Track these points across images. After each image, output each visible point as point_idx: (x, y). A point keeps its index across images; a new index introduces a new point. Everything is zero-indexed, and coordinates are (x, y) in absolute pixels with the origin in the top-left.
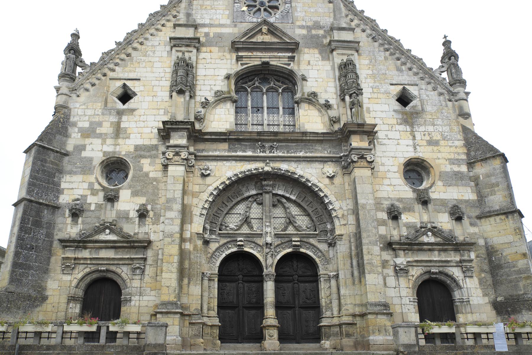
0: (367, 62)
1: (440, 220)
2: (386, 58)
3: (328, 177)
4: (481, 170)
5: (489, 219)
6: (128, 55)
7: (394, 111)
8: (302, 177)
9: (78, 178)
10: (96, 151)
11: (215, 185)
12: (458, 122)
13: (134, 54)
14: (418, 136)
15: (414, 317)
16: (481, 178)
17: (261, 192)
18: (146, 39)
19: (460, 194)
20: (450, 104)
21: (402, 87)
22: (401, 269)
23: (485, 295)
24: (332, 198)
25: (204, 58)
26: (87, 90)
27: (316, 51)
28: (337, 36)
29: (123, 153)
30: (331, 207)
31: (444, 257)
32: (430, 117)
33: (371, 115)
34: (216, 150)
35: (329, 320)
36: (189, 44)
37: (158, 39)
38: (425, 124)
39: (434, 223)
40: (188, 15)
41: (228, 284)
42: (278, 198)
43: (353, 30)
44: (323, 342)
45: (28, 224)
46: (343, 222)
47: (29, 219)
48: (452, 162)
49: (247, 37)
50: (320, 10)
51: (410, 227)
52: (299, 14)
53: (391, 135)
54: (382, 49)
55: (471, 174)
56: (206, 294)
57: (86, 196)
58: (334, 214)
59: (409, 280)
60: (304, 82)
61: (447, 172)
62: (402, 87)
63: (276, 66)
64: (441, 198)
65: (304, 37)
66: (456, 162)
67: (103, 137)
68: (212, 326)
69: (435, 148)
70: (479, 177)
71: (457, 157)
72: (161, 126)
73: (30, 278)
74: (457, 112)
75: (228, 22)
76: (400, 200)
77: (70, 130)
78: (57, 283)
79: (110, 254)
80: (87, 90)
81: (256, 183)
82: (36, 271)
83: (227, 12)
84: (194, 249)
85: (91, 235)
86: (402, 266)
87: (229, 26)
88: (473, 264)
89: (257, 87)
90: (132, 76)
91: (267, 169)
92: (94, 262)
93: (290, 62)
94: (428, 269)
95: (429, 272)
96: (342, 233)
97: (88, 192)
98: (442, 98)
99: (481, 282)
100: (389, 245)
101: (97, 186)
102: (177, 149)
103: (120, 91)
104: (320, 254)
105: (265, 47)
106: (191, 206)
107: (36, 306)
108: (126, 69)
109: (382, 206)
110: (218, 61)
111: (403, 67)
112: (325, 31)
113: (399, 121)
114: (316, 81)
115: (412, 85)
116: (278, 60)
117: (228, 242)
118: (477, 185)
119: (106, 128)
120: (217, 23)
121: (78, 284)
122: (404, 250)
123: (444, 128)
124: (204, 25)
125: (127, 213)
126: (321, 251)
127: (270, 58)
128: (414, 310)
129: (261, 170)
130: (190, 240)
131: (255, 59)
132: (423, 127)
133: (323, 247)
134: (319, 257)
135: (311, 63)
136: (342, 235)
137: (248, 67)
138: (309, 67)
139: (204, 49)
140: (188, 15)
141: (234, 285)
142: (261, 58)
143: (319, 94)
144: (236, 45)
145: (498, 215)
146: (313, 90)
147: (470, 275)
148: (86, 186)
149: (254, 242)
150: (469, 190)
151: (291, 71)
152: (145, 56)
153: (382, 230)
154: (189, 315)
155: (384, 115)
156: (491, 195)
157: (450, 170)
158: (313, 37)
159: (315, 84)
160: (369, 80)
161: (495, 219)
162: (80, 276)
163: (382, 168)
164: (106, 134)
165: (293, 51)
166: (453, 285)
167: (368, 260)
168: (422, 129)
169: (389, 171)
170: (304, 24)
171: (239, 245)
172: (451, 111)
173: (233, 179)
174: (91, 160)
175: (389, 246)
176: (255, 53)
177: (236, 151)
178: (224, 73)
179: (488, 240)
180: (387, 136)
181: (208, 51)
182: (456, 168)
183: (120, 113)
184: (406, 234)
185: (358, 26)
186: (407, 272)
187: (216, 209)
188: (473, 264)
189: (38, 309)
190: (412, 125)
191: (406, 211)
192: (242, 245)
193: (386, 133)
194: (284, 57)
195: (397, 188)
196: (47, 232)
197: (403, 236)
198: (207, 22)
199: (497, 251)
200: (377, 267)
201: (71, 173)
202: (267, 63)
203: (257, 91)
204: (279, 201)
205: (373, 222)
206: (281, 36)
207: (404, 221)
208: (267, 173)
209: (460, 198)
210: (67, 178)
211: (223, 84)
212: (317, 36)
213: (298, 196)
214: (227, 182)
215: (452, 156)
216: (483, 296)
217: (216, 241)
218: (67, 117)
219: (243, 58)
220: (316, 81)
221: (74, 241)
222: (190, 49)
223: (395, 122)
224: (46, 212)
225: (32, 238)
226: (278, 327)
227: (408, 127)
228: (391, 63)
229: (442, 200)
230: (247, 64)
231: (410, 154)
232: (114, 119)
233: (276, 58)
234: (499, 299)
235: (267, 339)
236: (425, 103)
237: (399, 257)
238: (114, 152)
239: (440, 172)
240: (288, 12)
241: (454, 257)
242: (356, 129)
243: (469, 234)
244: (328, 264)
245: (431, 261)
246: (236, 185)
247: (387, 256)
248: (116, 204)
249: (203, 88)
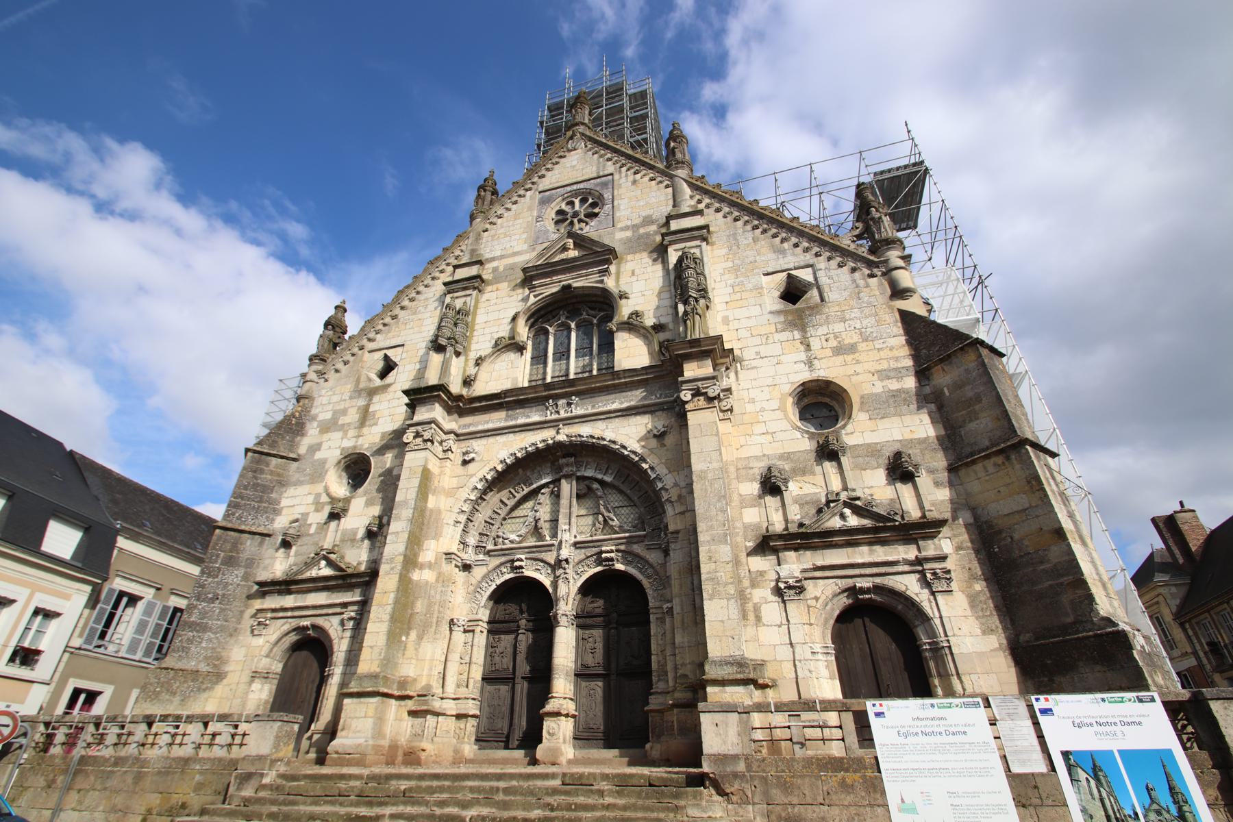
0: (725, 251)
1: (868, 483)
2: (755, 240)
3: (655, 436)
4: (943, 379)
5: (974, 467)
6: (394, 317)
7: (771, 313)
8: (614, 442)
9: (305, 489)
10: (333, 448)
11: (480, 475)
12: (891, 307)
13: (401, 314)
14: (815, 344)
15: (828, 687)
16: (947, 393)
17: (557, 476)
18: (418, 293)
19: (908, 430)
20: (873, 281)
21: (785, 274)
22: (790, 587)
23: (987, 631)
24: (662, 470)
26: (337, 371)
28: (675, 225)
29: (366, 446)
30: (660, 485)
31: (881, 553)
32: (837, 309)
33: (731, 327)
34: (487, 422)
35: (660, 699)
37: (433, 289)
38: (827, 322)
39: (854, 490)
40: (473, 251)
41: (503, 637)
42: (587, 482)
43: (700, 212)
44: (648, 746)
45: (216, 562)
46: (679, 509)
47: (218, 556)
48: (884, 375)
51: (807, 503)
53: (764, 351)
54: (749, 227)
55: (927, 390)
56: (454, 657)
57: (308, 514)
58: (665, 496)
59: (809, 607)
60: (624, 301)
61: (876, 395)
62: (785, 274)
64: (867, 442)
65: (629, 240)
66: (892, 374)
67: (343, 428)
68: (459, 717)
69: (849, 358)
70: (942, 392)
71: (893, 364)
72: (406, 400)
73: (204, 645)
74: (889, 292)
75: (525, 247)
76: (786, 457)
77: (308, 426)
78: (243, 651)
79: (320, 598)
80: (337, 371)
81: (553, 463)
82: (215, 633)
83: (525, 236)
84: (437, 581)
85: (300, 572)
86: (790, 581)
87: (525, 252)
88: (948, 564)
90: (394, 343)
91: (562, 437)
92: (296, 613)
94: (849, 583)
95: (852, 591)
96: (680, 526)
97: (312, 508)
98: (857, 275)
99: (973, 601)
100: (767, 545)
101: (325, 499)
102: (419, 428)
103: (380, 365)
104: (650, 571)
105: (569, 266)
106: (439, 512)
107: (205, 690)
108: (390, 335)
109: (751, 472)
111: (786, 245)
113: (779, 326)
115: (802, 268)
116: (583, 281)
117: (502, 564)
118: (940, 408)
119: (352, 416)
120: (510, 251)
121: (271, 650)
122: (796, 550)
123: (865, 322)
124: (493, 259)
125: (355, 532)
126: (651, 566)
128: (825, 673)
129: (550, 442)
130: (430, 566)
131: (550, 288)
132: (825, 327)
133: (654, 557)
134: (648, 577)
136: (677, 532)
138: (635, 278)
139: (489, 288)
140: (473, 251)
141: (511, 637)
145: (987, 457)
147: (945, 588)
148: (311, 499)
149: (542, 561)
150: (926, 419)
151: (605, 292)
152: (415, 313)
153: (752, 516)
154: (409, 697)
155: (752, 323)
156: (971, 421)
157: (881, 390)
158: (640, 237)
160: (727, 276)
161: (985, 467)
162: (274, 638)
163: (750, 408)
164: (349, 424)
166: (910, 614)
167: (709, 573)
168: (822, 330)
169: (763, 410)
170: (629, 223)
171: (517, 568)
172: (877, 293)
173: (508, 461)
174: (323, 462)
175: (767, 545)
177: (516, 419)
179: (979, 511)
180: (758, 353)
182: (894, 385)
183: (372, 392)
184: (798, 517)
185: (707, 206)
186: (800, 590)
187: (490, 512)
188: (948, 564)
189: (205, 695)
190: (803, 328)
191: (796, 475)
192: (521, 567)
193: (756, 349)
195: (779, 436)
196: (246, 573)
197: (793, 522)
198: (498, 253)
199: (1000, 532)
200: (726, 584)
201: (299, 483)
202: (569, 286)
204: (589, 488)
205: (719, 501)
207: (794, 493)
208: (559, 445)
209: (908, 436)
210: (291, 491)
212: (648, 235)
213: (618, 475)
214: (500, 468)
215: (885, 365)
216: (984, 633)
217: (483, 564)
218: (306, 411)
221: (274, 583)
222: (468, 292)
223: (773, 328)
224: (248, 543)
225: (218, 583)
226: (574, 716)
227: (796, 332)
228: (764, 243)
229: (869, 445)
231: (805, 375)
232: (362, 402)
234: (1022, 638)
235: (544, 740)
236: (826, 289)
237: (787, 562)
238: (355, 447)
239: (862, 397)
241: (911, 553)
243: (933, 505)
244: (664, 588)
245: (852, 566)
246: (520, 471)
247: (759, 563)
248: (343, 520)
249: (481, 339)
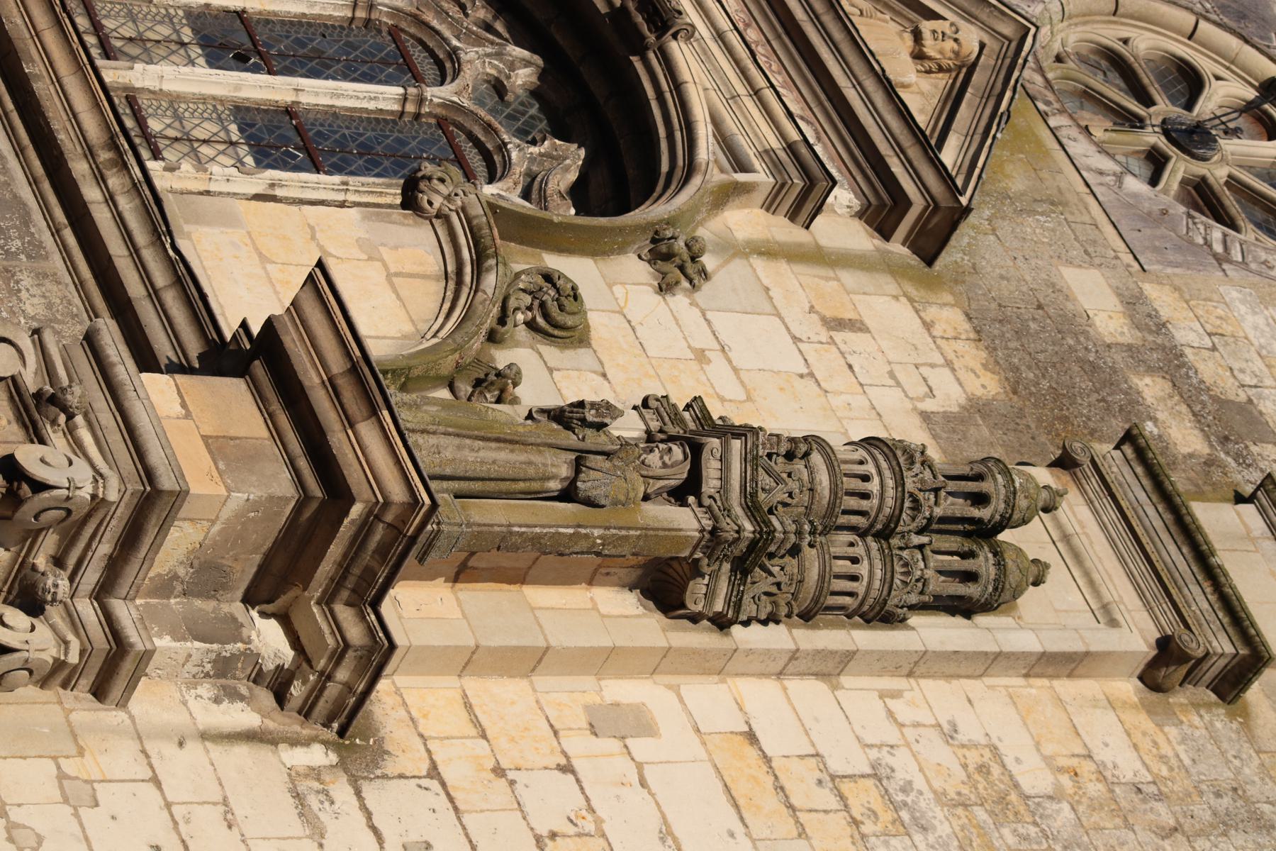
63: (678, 87)
233: (743, 72)
242: (311, 378)
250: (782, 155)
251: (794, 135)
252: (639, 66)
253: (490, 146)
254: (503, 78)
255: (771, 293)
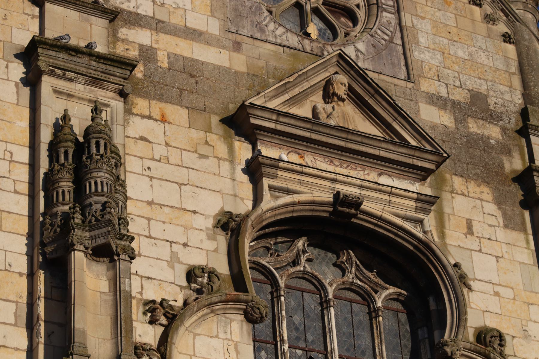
25: (142, 138)
27: (486, 193)
36: (104, 76)
49: (286, 97)
50: (482, 58)
52: (426, 56)
63: (380, 218)
89: (305, 276)
93: (421, 216)
110: (190, 159)
112: (504, 130)
114: (497, 294)
116: (387, 198)
120: (176, 20)
124: (136, 20)
127: (361, 187)
131: (312, 181)
135: (476, 227)
137: (293, 204)
138: (471, 243)
142: (334, 181)
143: (508, 338)
144: (257, 117)
146: (491, 323)
159: (493, 304)
165: (423, 174)
170: (443, 92)
176: (309, 159)
178: (212, 205)
181: (156, 114)
194: (404, 194)
202: (356, 204)
203: (302, 291)
206: (389, 119)
211: (210, 245)
219: (277, 167)
220: (497, 294)
230: (288, 192)
233: (380, 191)
240: (391, 41)
250: (419, 205)
251: (415, 196)
252: (356, 221)
253: (348, 287)
254: (308, 257)
255: (461, 246)
